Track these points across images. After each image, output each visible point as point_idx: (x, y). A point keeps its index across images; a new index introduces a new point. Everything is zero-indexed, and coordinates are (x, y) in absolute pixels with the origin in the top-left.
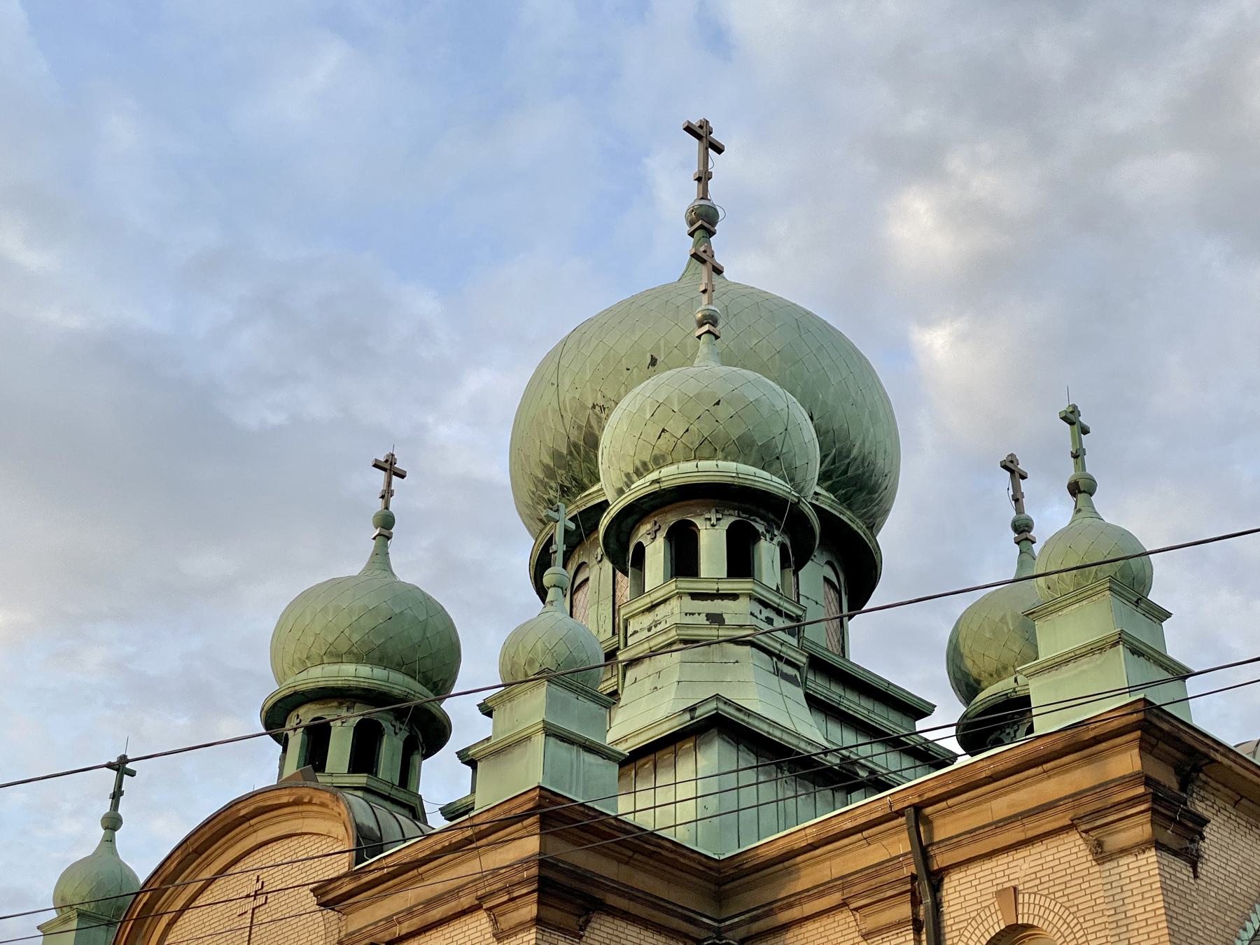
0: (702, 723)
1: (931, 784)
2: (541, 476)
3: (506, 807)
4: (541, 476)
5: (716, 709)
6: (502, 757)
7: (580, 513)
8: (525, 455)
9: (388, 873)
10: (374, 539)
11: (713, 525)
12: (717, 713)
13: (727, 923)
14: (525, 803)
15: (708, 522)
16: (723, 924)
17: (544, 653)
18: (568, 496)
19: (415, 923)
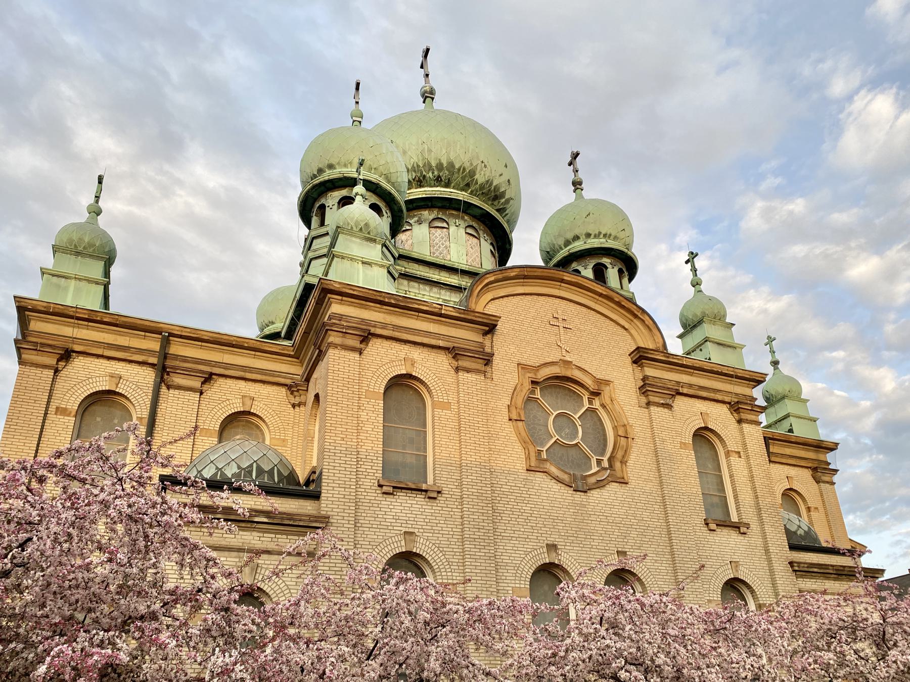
1: (777, 434)
2: (434, 164)
4: (434, 164)
6: (721, 347)
8: (428, 148)
19: (691, 392)
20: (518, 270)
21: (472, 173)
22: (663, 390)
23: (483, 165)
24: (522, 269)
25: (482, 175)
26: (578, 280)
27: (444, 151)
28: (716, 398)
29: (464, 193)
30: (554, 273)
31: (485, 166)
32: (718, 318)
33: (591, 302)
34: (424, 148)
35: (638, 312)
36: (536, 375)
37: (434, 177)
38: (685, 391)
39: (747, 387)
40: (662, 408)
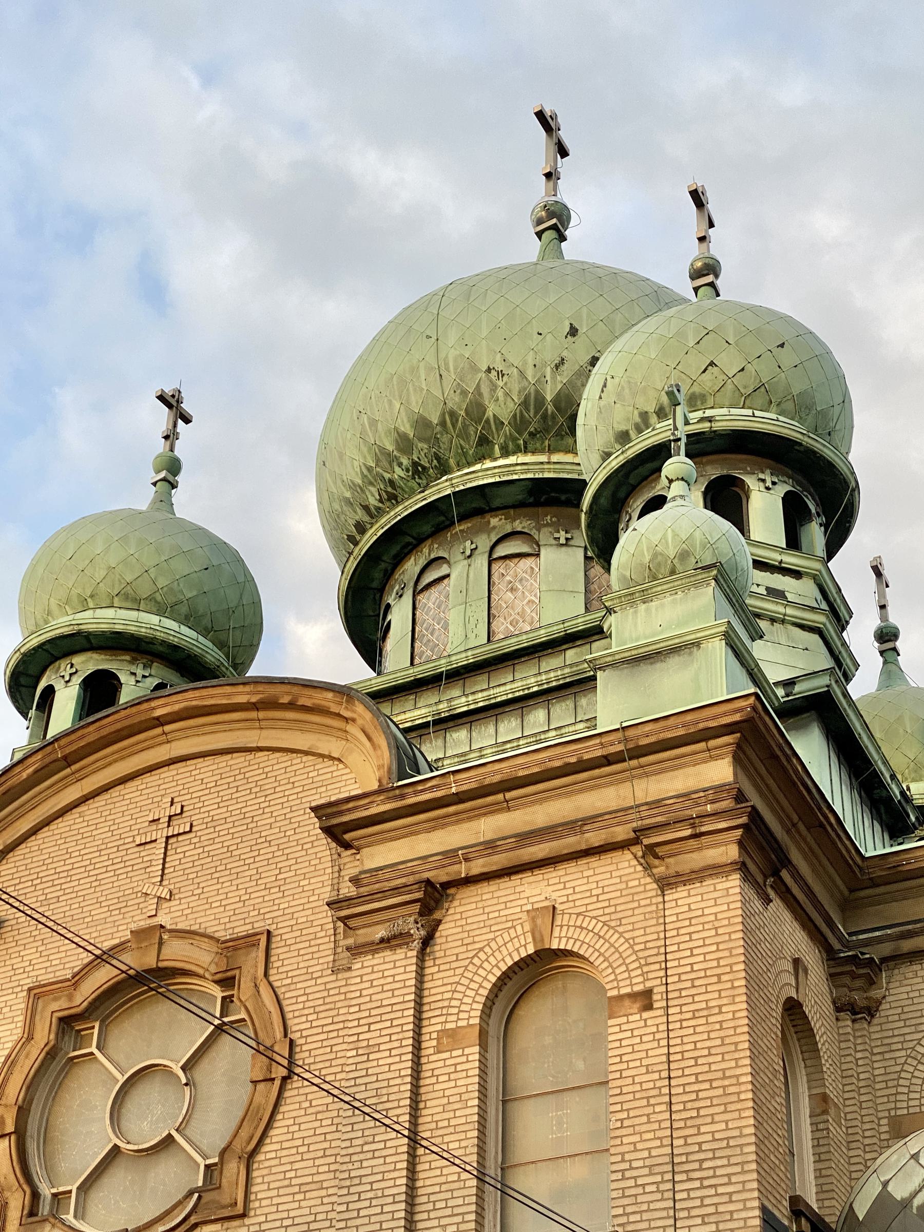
0: (798, 702)
2: (390, 447)
3: (689, 717)
4: (390, 447)
5: (827, 686)
7: (454, 493)
8: (369, 418)
9: (457, 793)
10: (155, 484)
11: (768, 488)
12: (829, 691)
13: (861, 937)
14: (725, 714)
15: (761, 484)
16: (854, 938)
17: (703, 546)
18: (420, 478)
20: (39, 756)
21: (476, 410)
22: (386, 898)
23: (494, 373)
24: (49, 749)
25: (501, 398)
26: (187, 700)
27: (397, 405)
28: (584, 847)
29: (488, 464)
30: (127, 717)
31: (500, 374)
32: (665, 570)
33: (248, 733)
34: (363, 425)
35: (340, 704)
36: (70, 998)
37: (408, 470)
38: (477, 867)
39: (712, 758)
40: (388, 953)
